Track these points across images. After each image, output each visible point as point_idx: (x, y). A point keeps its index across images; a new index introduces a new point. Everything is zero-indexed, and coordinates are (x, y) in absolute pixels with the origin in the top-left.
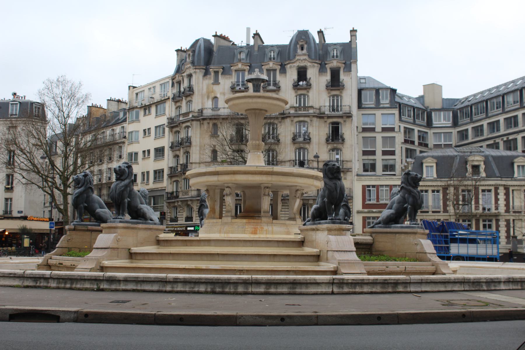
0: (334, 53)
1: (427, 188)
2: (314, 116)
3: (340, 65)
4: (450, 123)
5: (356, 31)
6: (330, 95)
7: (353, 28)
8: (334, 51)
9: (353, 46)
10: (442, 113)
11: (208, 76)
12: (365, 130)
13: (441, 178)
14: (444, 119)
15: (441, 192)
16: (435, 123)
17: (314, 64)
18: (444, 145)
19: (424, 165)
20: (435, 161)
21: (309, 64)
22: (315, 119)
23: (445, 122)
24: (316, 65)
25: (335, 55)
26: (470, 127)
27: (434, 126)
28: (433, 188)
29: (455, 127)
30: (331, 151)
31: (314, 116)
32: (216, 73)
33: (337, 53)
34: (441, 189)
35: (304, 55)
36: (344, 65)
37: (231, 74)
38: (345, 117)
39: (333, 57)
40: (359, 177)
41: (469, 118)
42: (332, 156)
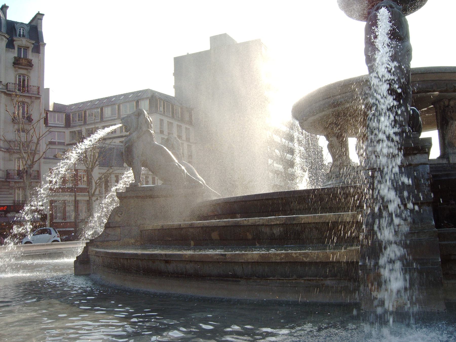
0: (20, 32)
3: (29, 44)
4: (63, 124)
5: (43, 15)
6: (16, 73)
7: (39, 12)
8: (20, 30)
9: (39, 29)
10: (56, 114)
14: (58, 120)
16: (50, 122)
17: (3, 37)
18: (58, 142)
23: (58, 123)
24: (5, 39)
25: (22, 33)
26: (84, 129)
27: (49, 125)
29: (67, 128)
30: (17, 131)
33: (23, 33)
36: (33, 46)
38: (34, 98)
39: (20, 35)
40: (45, 160)
41: (83, 121)
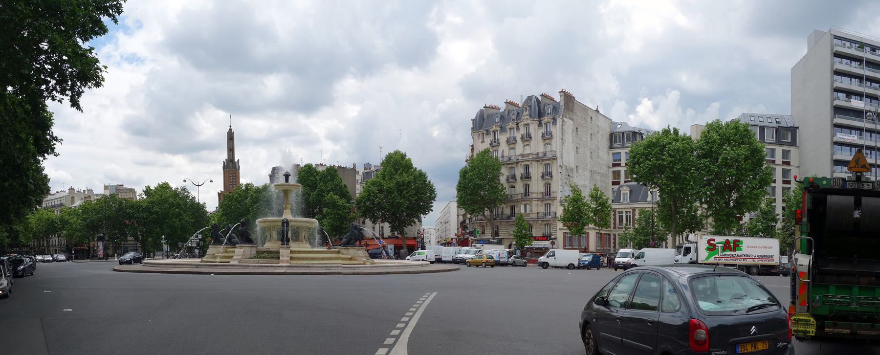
1: (622, 210)
2: (532, 160)
11: (489, 136)
12: (614, 165)
13: (632, 202)
15: (631, 213)
19: (622, 192)
20: (628, 188)
21: (530, 122)
22: (534, 162)
28: (626, 210)
31: (532, 160)
32: (483, 134)
34: (631, 210)
35: (527, 115)
36: (552, 120)
37: (506, 132)
42: (547, 190)
